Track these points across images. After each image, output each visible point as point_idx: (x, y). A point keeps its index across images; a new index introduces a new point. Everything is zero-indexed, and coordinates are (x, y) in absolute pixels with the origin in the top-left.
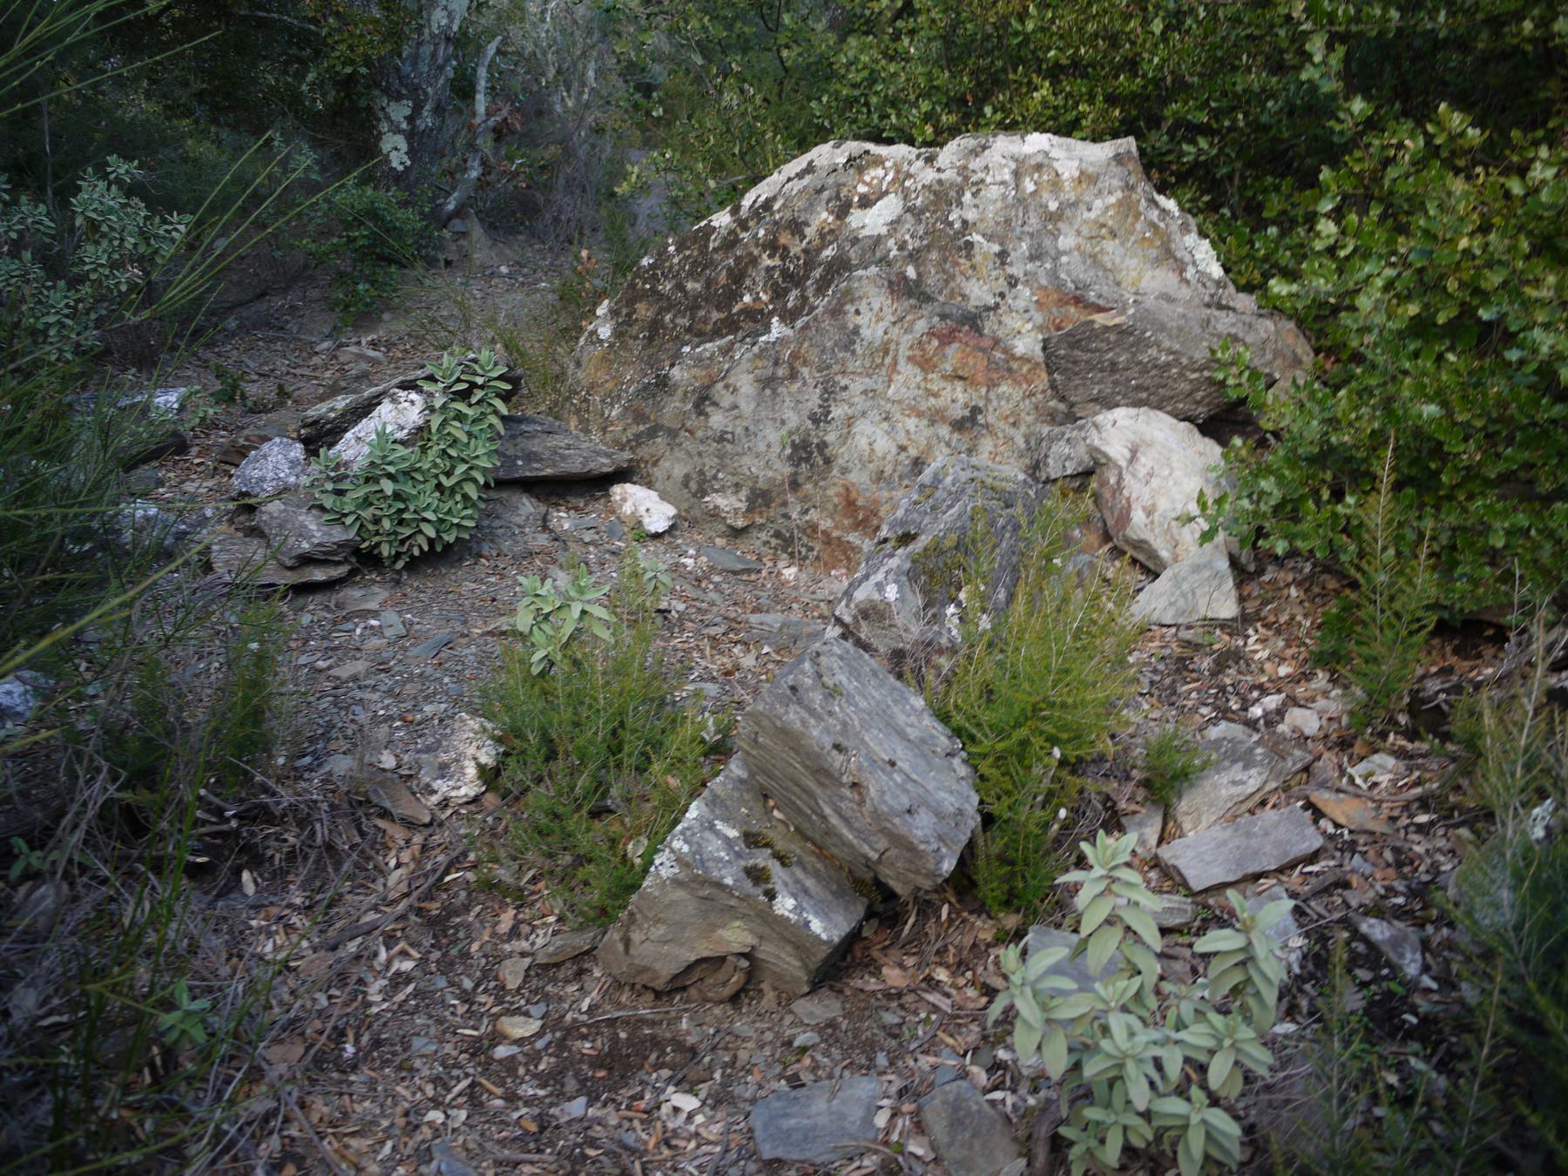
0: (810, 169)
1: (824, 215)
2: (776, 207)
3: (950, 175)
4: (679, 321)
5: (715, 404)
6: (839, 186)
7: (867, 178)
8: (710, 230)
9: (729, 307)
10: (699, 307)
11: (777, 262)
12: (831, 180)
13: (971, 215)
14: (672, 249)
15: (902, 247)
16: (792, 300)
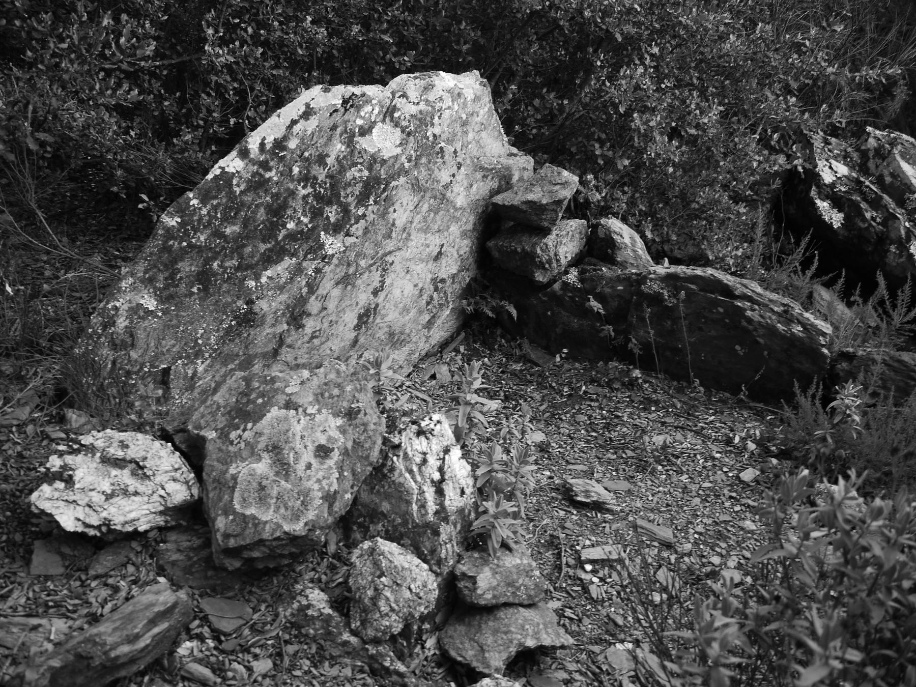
0: (308, 113)
1: (339, 146)
2: (293, 144)
3: (422, 106)
4: (227, 264)
5: (309, 315)
6: (346, 122)
7: (362, 114)
8: (226, 178)
9: (276, 236)
10: (244, 246)
11: (309, 190)
12: (337, 117)
13: (437, 130)
14: (194, 202)
15: (409, 161)
16: (332, 213)
